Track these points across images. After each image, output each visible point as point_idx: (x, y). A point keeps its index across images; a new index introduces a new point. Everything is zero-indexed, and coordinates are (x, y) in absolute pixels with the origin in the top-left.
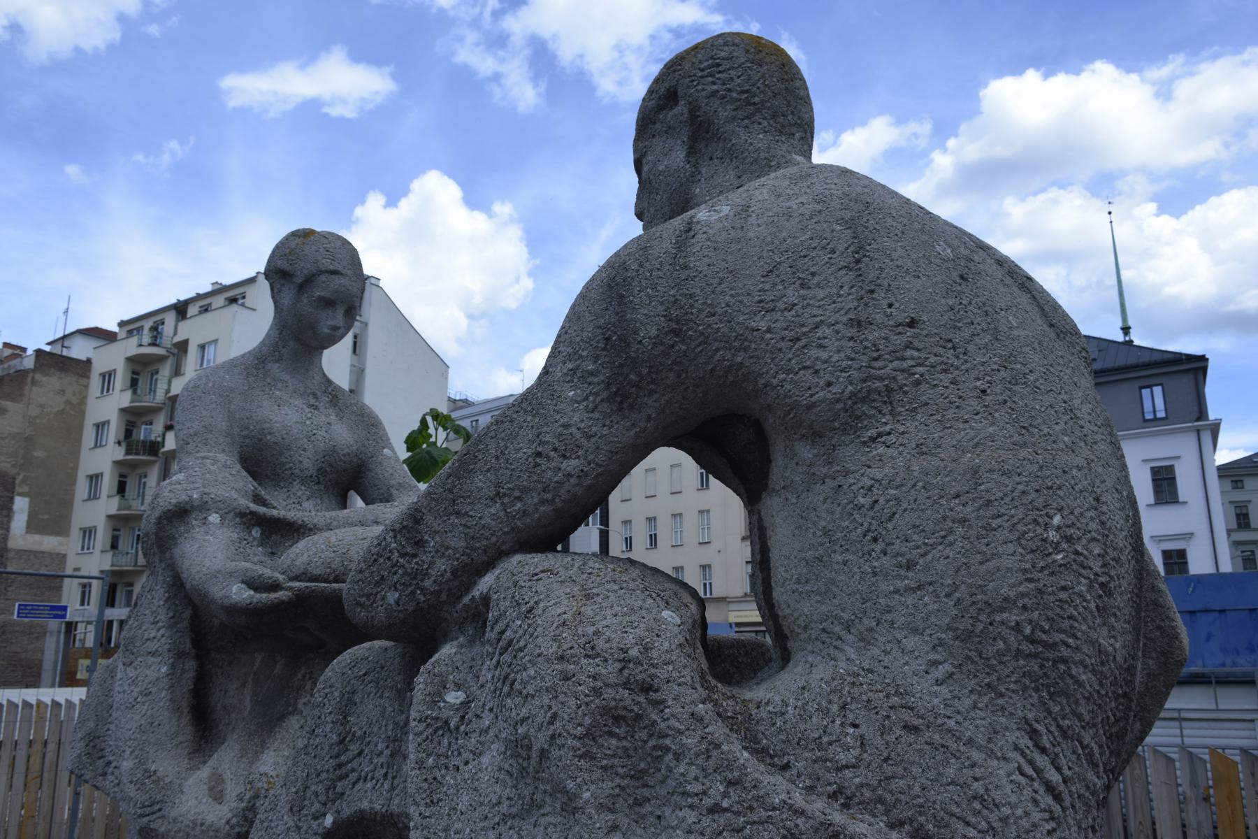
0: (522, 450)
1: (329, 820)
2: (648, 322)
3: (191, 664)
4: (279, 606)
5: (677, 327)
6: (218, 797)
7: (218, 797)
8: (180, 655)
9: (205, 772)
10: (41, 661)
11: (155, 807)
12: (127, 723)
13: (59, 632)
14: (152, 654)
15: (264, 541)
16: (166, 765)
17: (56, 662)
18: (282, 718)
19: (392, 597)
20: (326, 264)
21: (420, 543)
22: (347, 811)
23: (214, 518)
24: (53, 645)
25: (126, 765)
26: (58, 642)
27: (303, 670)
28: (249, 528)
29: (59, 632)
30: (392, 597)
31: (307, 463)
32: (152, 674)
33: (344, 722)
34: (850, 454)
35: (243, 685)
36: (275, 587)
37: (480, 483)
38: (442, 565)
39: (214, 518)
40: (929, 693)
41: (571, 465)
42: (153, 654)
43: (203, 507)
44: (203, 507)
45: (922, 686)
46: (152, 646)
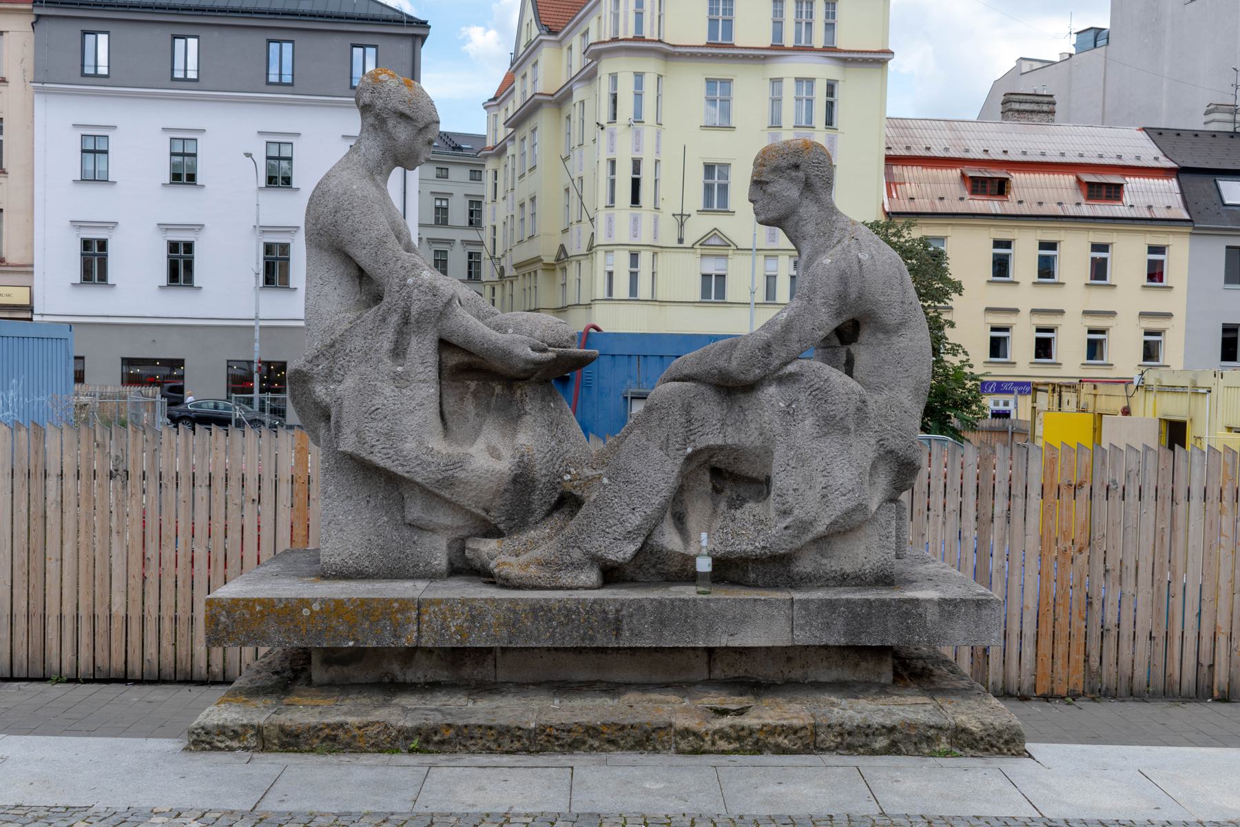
0: (808, 327)
1: (689, 450)
2: (853, 293)
4: (554, 360)
7: (499, 458)
14: (424, 381)
18: (519, 416)
19: (757, 371)
21: (770, 354)
22: (699, 446)
27: (519, 392)
30: (757, 371)
32: (424, 394)
33: (688, 413)
34: (895, 339)
35: (462, 399)
37: (794, 336)
38: (777, 362)
41: (821, 333)
42: (424, 381)
45: (906, 401)
46: (422, 377)
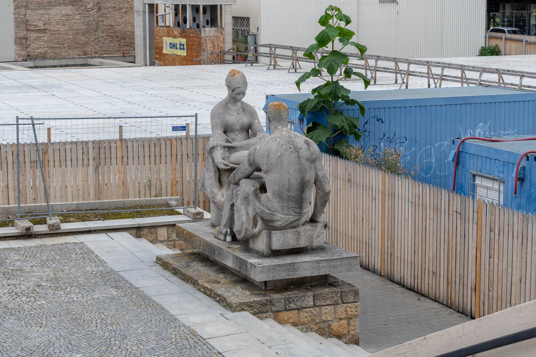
3: (218, 173)
5: (254, 161)
6: (223, 197)
7: (223, 197)
8: (216, 172)
9: (221, 193)
10: (133, 32)
11: (214, 197)
12: (207, 183)
13: (144, 12)
15: (228, 151)
16: (216, 190)
17: (145, 38)
20: (237, 86)
23: (219, 148)
24: (141, 24)
25: (209, 190)
26: (144, 21)
28: (225, 149)
29: (144, 12)
31: (238, 127)
36: (228, 166)
39: (219, 148)
40: (271, 198)
43: (217, 146)
44: (217, 146)
